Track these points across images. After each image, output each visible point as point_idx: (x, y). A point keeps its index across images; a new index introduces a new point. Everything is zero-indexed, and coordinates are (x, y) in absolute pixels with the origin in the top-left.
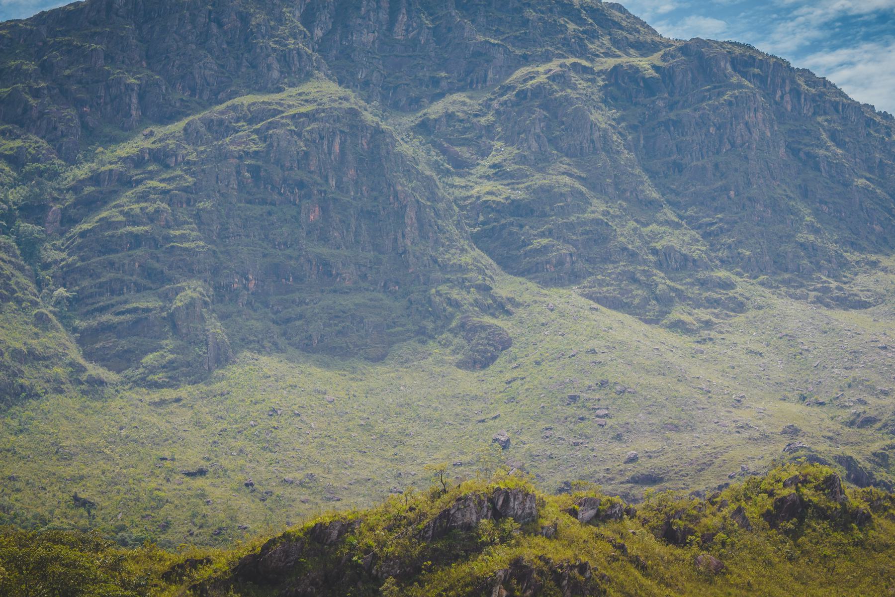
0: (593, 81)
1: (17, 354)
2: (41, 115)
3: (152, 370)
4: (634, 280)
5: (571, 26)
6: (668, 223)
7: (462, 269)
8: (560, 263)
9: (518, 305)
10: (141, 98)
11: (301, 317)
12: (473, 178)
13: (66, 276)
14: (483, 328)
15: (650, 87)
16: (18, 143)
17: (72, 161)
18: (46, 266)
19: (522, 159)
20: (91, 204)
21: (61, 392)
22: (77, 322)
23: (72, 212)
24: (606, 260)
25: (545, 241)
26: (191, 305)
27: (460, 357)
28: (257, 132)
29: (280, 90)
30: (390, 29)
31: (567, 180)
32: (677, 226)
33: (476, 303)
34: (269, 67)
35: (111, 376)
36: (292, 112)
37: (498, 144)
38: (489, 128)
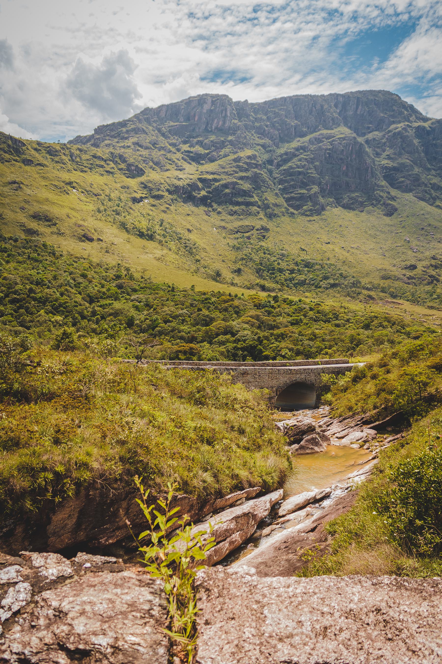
0: (412, 130)
1: (273, 204)
2: (268, 133)
3: (306, 211)
4: (426, 192)
5: (406, 112)
6: (433, 175)
7: (382, 186)
8: (407, 186)
9: (397, 198)
10: (295, 129)
11: (342, 198)
12: (381, 159)
13: (281, 182)
14: (390, 204)
15: (428, 133)
16: (263, 141)
17: (278, 147)
18: (275, 179)
19: (395, 154)
20: (285, 161)
21: (284, 216)
22: (285, 196)
23: (280, 163)
24: (419, 185)
25: (403, 179)
26: (315, 193)
27: (384, 212)
28: (329, 142)
29: (332, 129)
30: (356, 111)
31: (408, 161)
32: (436, 176)
33: (387, 197)
34: (329, 122)
35: (295, 212)
36: (338, 137)
37: (388, 149)
38: (385, 143)
